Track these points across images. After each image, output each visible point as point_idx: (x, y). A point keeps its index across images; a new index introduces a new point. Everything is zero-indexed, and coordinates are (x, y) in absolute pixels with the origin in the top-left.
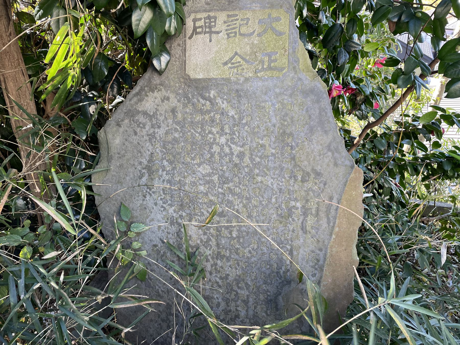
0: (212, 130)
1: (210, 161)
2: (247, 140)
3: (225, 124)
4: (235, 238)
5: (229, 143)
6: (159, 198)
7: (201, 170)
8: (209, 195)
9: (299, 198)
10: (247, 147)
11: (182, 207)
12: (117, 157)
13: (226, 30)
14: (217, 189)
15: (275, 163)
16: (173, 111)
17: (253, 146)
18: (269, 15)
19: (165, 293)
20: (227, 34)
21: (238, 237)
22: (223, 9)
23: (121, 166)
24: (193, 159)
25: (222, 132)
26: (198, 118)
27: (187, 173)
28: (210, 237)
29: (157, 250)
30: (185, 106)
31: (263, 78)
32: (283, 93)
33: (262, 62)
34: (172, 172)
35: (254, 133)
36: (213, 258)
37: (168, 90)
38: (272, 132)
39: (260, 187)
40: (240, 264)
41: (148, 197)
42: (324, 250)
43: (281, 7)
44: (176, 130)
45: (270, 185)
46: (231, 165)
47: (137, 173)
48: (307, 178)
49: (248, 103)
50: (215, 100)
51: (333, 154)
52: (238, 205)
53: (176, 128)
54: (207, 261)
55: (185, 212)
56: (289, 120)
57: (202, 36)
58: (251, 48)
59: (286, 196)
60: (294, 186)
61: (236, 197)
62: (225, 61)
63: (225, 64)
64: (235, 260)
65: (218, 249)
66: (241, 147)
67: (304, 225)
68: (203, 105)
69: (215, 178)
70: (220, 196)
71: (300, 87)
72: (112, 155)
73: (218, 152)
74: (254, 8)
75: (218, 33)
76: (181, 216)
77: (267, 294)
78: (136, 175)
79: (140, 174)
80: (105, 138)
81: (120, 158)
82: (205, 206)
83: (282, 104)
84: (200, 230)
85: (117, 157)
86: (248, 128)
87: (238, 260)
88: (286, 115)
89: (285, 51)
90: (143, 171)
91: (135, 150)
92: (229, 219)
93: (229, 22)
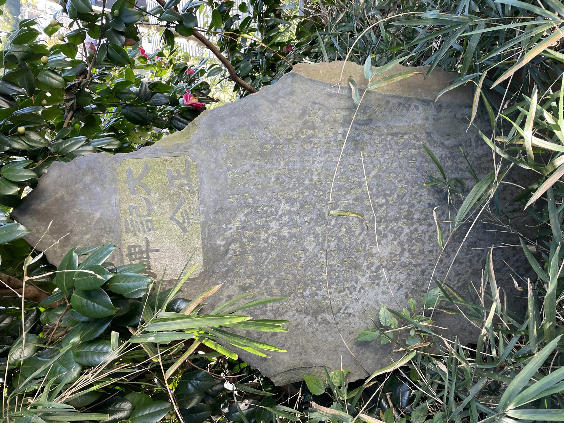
0: (263, 239)
1: (300, 238)
2: (272, 196)
3: (255, 223)
4: (387, 200)
5: (277, 217)
6: (350, 296)
7: (312, 248)
8: (340, 235)
9: (333, 131)
10: (280, 195)
11: (357, 267)
12: (305, 355)
13: (144, 232)
14: (332, 226)
15: (296, 161)
16: (244, 289)
17: (278, 189)
18: (125, 183)
19: (460, 278)
20: (148, 232)
21: (385, 196)
22: (120, 239)
23: (316, 349)
24: (299, 259)
25: (265, 227)
26: (250, 257)
27: (316, 265)
28: (388, 229)
29: (411, 292)
30: (237, 275)
31: (199, 184)
32: (216, 159)
33: (180, 187)
34: (317, 283)
35: (264, 188)
36: (413, 224)
37: (219, 298)
38: (261, 167)
39: (325, 176)
40: (415, 191)
41: (350, 311)
42: (387, 99)
43: (115, 170)
44: (267, 283)
45: (322, 165)
46: (303, 213)
47: (323, 327)
48: (310, 123)
49: (229, 198)
50: (228, 238)
51: (280, 97)
52: (348, 200)
53: (265, 284)
54: (416, 230)
55: (363, 263)
56: (246, 150)
57: (152, 262)
58: (165, 201)
59: (333, 146)
60: (320, 138)
61: (339, 203)
62: (181, 230)
63: (184, 229)
64: (412, 198)
65: (401, 218)
66: (281, 202)
67: (363, 122)
68: (235, 252)
69: (319, 230)
70: (339, 222)
71: (207, 140)
72: (304, 363)
73: (289, 229)
74: (117, 201)
75: (148, 242)
76: (368, 267)
77: (445, 158)
78: (324, 329)
79: (323, 323)
80: (282, 375)
81: (305, 352)
82: (354, 239)
83: (228, 158)
84: (382, 242)
85: (305, 355)
86: (258, 196)
87: (411, 195)
88: (240, 153)
89: (167, 160)
90: (319, 320)
91: (295, 333)
92: (365, 208)
93: (134, 229)
